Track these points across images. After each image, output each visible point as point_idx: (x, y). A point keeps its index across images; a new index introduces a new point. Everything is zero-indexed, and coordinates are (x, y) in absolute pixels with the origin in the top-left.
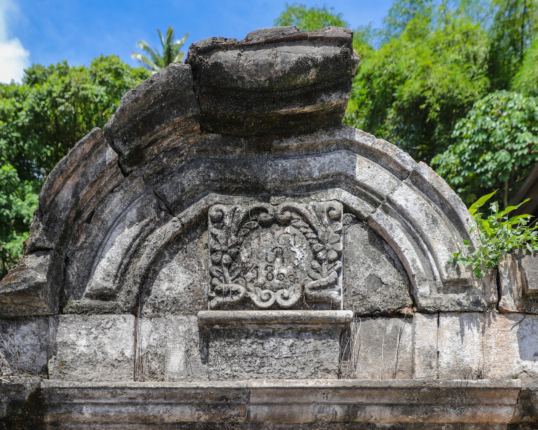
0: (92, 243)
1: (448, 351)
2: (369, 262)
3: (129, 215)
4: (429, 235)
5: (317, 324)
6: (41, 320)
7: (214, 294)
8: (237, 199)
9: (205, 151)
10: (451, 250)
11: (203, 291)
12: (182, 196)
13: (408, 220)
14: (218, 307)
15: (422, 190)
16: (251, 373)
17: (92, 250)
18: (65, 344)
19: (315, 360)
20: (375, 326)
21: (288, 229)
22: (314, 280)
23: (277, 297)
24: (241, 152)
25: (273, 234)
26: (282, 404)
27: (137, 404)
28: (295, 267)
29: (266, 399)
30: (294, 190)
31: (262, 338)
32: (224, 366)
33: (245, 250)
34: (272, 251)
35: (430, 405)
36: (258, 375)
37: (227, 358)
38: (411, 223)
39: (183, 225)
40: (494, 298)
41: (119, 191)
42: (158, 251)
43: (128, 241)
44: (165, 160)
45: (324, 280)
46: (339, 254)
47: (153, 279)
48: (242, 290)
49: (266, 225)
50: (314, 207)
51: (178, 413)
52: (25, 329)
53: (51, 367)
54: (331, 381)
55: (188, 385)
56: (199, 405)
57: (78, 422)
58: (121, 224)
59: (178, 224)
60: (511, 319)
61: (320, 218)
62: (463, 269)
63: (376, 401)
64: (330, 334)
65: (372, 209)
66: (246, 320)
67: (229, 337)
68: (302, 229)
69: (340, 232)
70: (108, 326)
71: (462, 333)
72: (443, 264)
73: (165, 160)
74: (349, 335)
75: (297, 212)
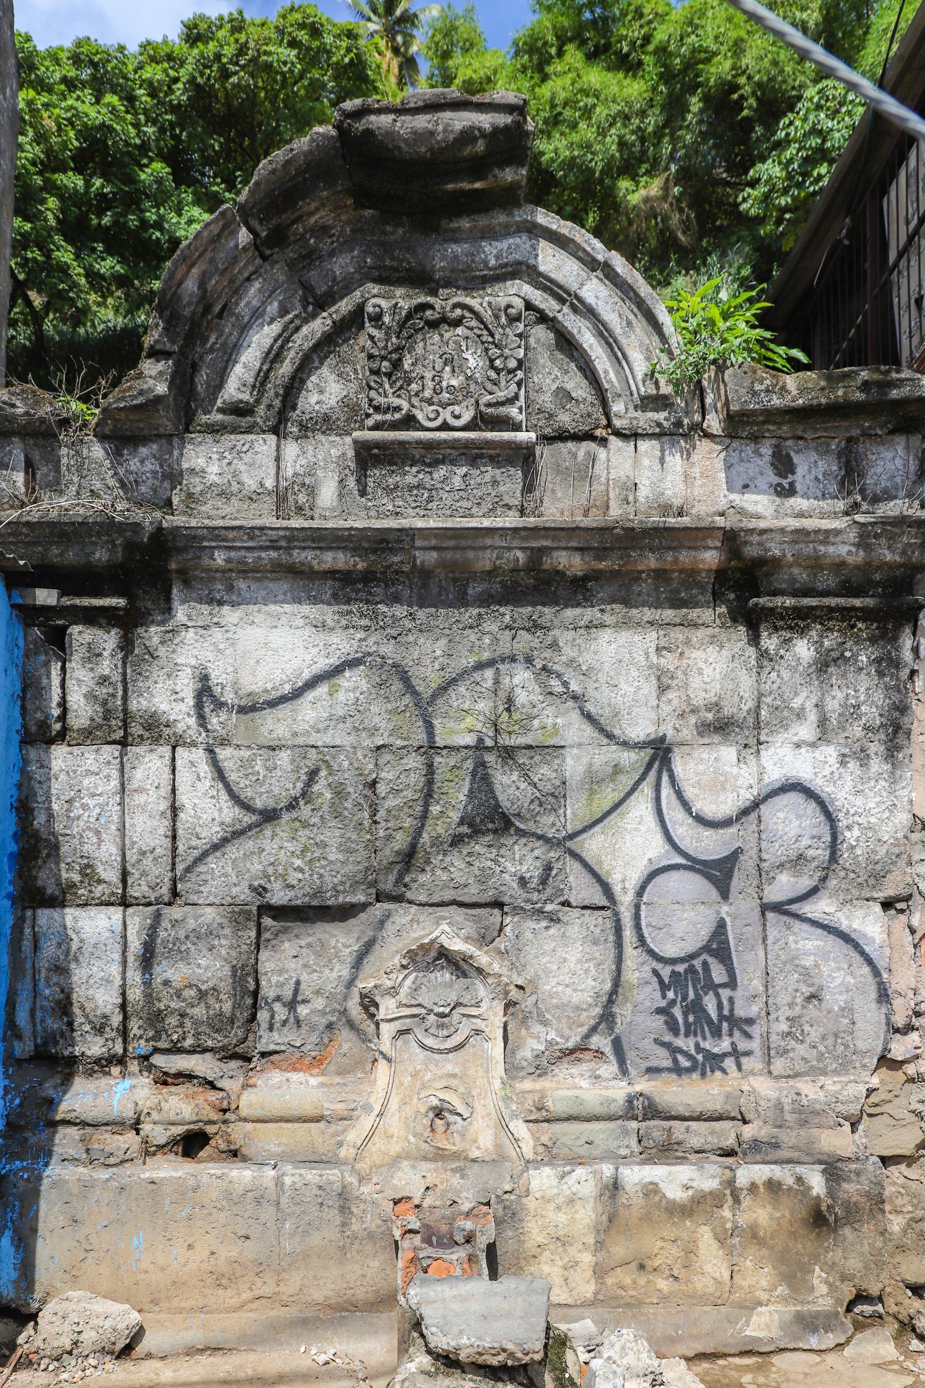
0: (225, 344)
1: (647, 483)
2: (556, 372)
3: (269, 309)
4: (623, 341)
5: (495, 449)
6: (164, 441)
7: (371, 411)
8: (399, 292)
9: (361, 230)
10: (648, 359)
11: (359, 406)
12: (333, 286)
13: (599, 321)
14: (377, 427)
15: (615, 285)
16: (418, 510)
17: (225, 353)
18: (192, 471)
19: (494, 494)
20: (564, 451)
21: (460, 330)
22: (491, 394)
23: (446, 415)
24: (404, 233)
25: (442, 336)
26: (454, 548)
27: (280, 548)
28: (468, 378)
29: (434, 542)
30: (467, 281)
31: (430, 465)
32: (385, 501)
33: (408, 356)
34: (441, 357)
35: (626, 548)
36: (425, 512)
37: (390, 491)
38: (603, 325)
39: (334, 322)
40: (697, 417)
41: (257, 279)
42: (304, 355)
43: (268, 342)
44: (312, 241)
45: (502, 394)
46: (520, 363)
47: (300, 390)
48: (405, 405)
49: (433, 325)
50: (490, 303)
51: (329, 559)
52: (144, 451)
53: (175, 500)
54: (511, 520)
55: (342, 524)
56: (354, 549)
57: (210, 570)
58: (260, 321)
59: (329, 322)
60: (717, 443)
61: (497, 317)
62: (662, 382)
63: (563, 544)
64: (510, 462)
65: (558, 308)
66: (409, 443)
67: (390, 464)
68: (476, 331)
69: (520, 336)
70: (244, 449)
71: (662, 461)
72: (640, 376)
73: (312, 241)
74: (534, 462)
75: (470, 309)
